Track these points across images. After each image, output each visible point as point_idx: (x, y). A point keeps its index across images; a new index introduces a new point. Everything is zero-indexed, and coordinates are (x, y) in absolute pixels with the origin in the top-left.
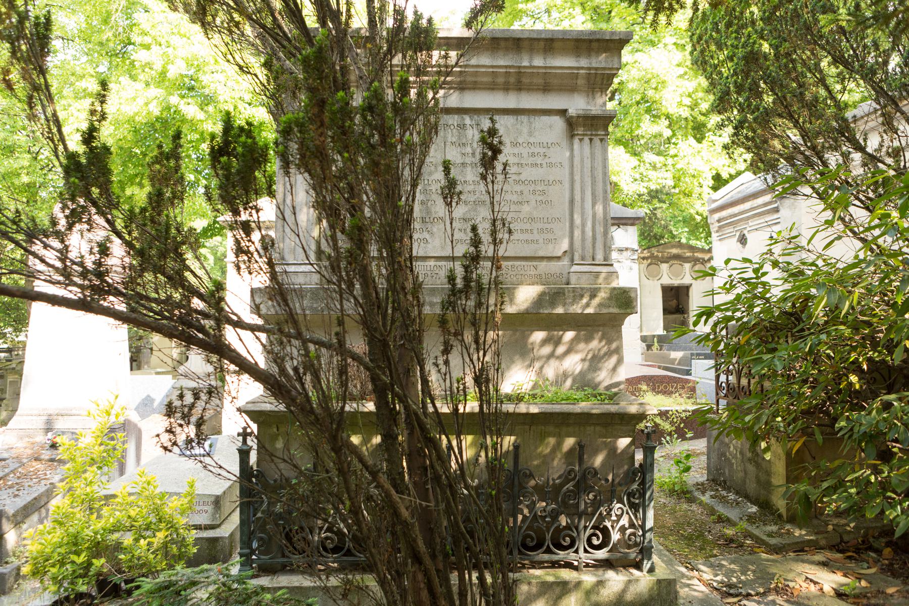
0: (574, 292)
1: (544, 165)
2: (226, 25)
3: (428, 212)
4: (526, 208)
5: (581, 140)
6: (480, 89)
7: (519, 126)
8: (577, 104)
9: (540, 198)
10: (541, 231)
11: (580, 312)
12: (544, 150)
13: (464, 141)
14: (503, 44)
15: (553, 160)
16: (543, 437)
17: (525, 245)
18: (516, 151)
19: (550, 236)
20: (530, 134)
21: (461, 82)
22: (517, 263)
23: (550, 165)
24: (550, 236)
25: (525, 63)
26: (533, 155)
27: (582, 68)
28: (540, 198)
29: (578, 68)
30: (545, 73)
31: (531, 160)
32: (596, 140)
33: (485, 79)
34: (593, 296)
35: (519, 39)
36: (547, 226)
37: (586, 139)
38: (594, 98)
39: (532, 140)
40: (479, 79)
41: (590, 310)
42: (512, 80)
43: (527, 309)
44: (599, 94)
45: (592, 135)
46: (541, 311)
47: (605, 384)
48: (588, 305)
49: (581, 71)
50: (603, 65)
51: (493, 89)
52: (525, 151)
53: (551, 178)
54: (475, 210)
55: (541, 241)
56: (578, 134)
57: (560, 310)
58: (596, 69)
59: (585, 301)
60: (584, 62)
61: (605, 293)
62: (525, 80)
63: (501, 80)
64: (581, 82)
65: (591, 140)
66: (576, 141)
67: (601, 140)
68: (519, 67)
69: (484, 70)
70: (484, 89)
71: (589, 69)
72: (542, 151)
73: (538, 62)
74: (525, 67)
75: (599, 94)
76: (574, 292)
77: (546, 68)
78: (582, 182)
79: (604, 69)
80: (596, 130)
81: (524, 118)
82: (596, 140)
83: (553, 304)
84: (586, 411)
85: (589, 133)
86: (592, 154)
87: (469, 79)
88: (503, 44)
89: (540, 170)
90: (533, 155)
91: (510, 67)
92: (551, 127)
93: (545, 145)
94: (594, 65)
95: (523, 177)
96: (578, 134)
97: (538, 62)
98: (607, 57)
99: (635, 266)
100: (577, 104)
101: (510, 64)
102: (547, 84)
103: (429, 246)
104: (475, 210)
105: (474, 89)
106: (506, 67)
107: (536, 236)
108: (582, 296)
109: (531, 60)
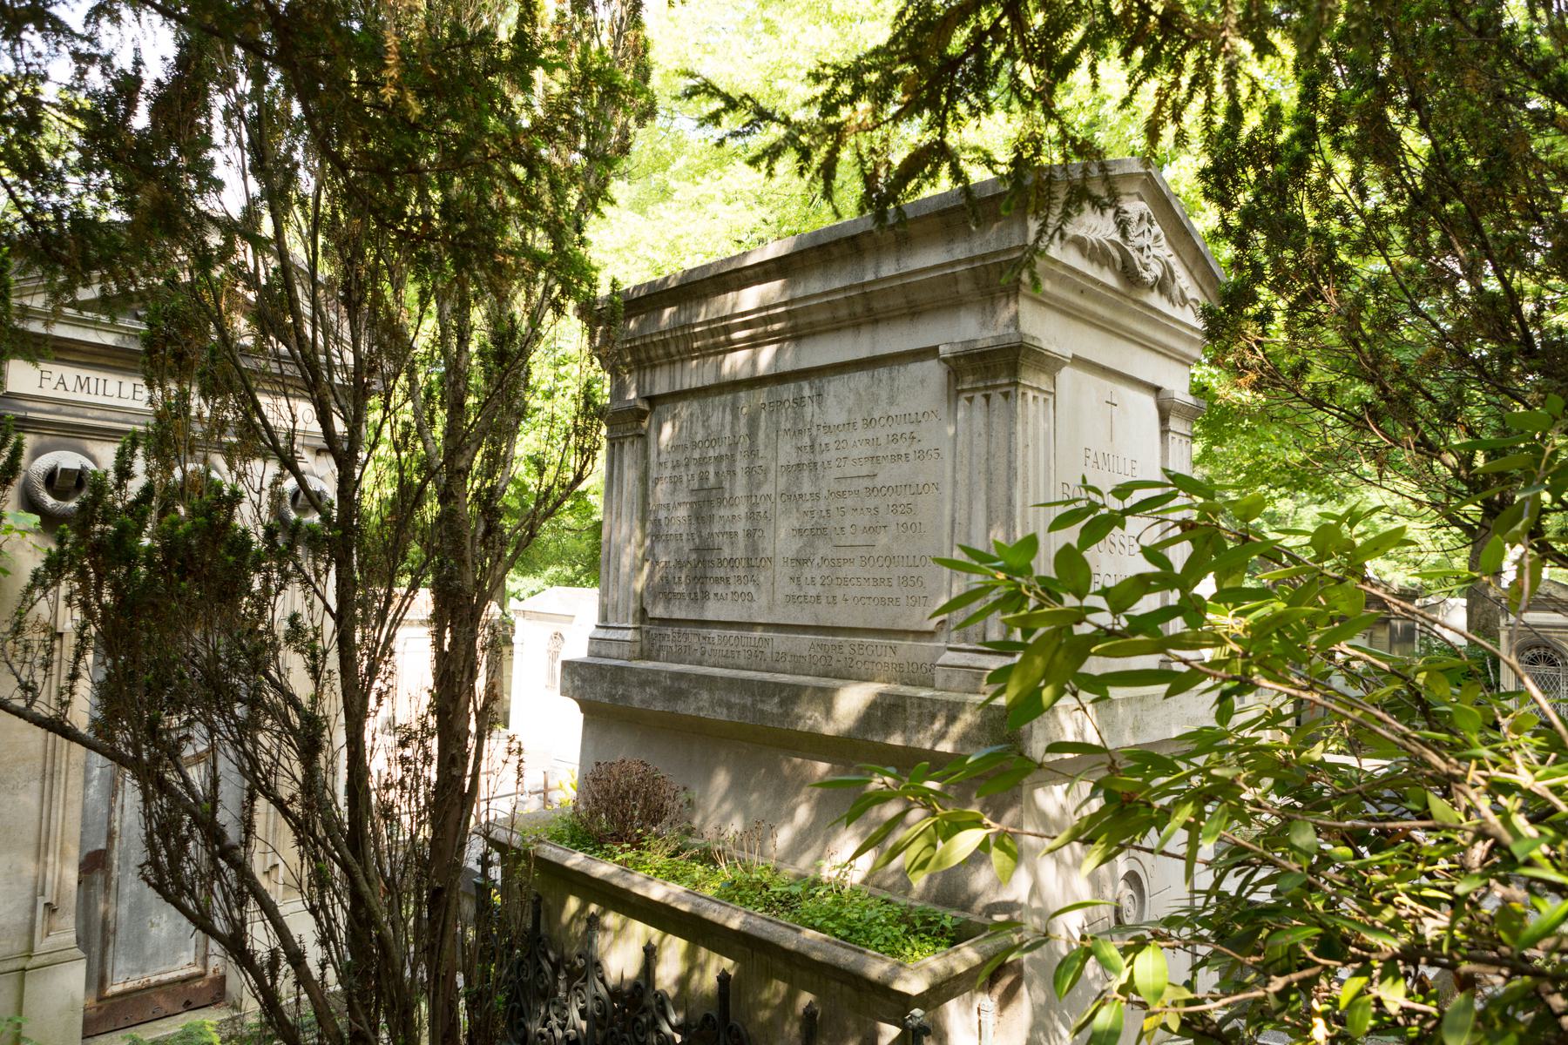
0: (920, 706)
1: (911, 457)
2: (784, 229)
3: (755, 550)
4: (883, 539)
5: (970, 400)
6: (821, 333)
7: (874, 389)
8: (967, 330)
9: (903, 519)
10: (905, 581)
11: (928, 746)
12: (912, 428)
13: (800, 426)
14: (835, 251)
15: (924, 445)
16: (769, 975)
17: (880, 607)
18: (870, 434)
19: (918, 592)
20: (892, 401)
21: (794, 329)
22: (867, 640)
23: (921, 454)
24: (918, 592)
25: (870, 277)
26: (894, 439)
27: (959, 262)
28: (903, 519)
29: (952, 264)
30: (903, 285)
31: (892, 449)
32: (997, 399)
33: (823, 316)
34: (951, 719)
35: (853, 238)
36: (914, 572)
37: (979, 399)
38: (994, 312)
39: (894, 411)
40: (816, 317)
41: (946, 747)
42: (859, 309)
43: (849, 731)
44: (1004, 301)
45: (987, 388)
46: (869, 737)
47: (983, 901)
48: (941, 736)
49: (959, 269)
50: (993, 247)
51: (838, 329)
52: (882, 433)
53: (921, 480)
54: (812, 546)
55: (903, 601)
56: (963, 391)
57: (896, 740)
58: (983, 257)
59: (937, 726)
60: (960, 251)
61: (973, 714)
62: (877, 305)
63: (843, 312)
64: (964, 287)
65: (987, 397)
66: (962, 402)
67: (1006, 395)
68: (863, 285)
69: (815, 302)
70: (827, 331)
71: (971, 260)
72: (906, 429)
73: (888, 269)
74: (870, 283)
75: (1004, 301)
76: (920, 706)
77: (901, 276)
78: (970, 484)
79: (996, 253)
80: (995, 377)
81: (883, 373)
82: (997, 399)
83: (888, 729)
84: (802, 950)
85: (981, 384)
86: (989, 425)
87: (802, 321)
88: (835, 251)
89: (905, 466)
90: (894, 439)
91: (851, 287)
92: (922, 382)
93: (913, 417)
94: (978, 251)
95: (878, 482)
96: (963, 391)
97: (888, 269)
98: (1000, 229)
99: (238, 791)
100: (967, 330)
101: (845, 283)
102: (914, 303)
103: (755, 605)
104: (812, 546)
105: (814, 334)
106: (845, 289)
107: (896, 591)
108: (933, 717)
109: (878, 267)
